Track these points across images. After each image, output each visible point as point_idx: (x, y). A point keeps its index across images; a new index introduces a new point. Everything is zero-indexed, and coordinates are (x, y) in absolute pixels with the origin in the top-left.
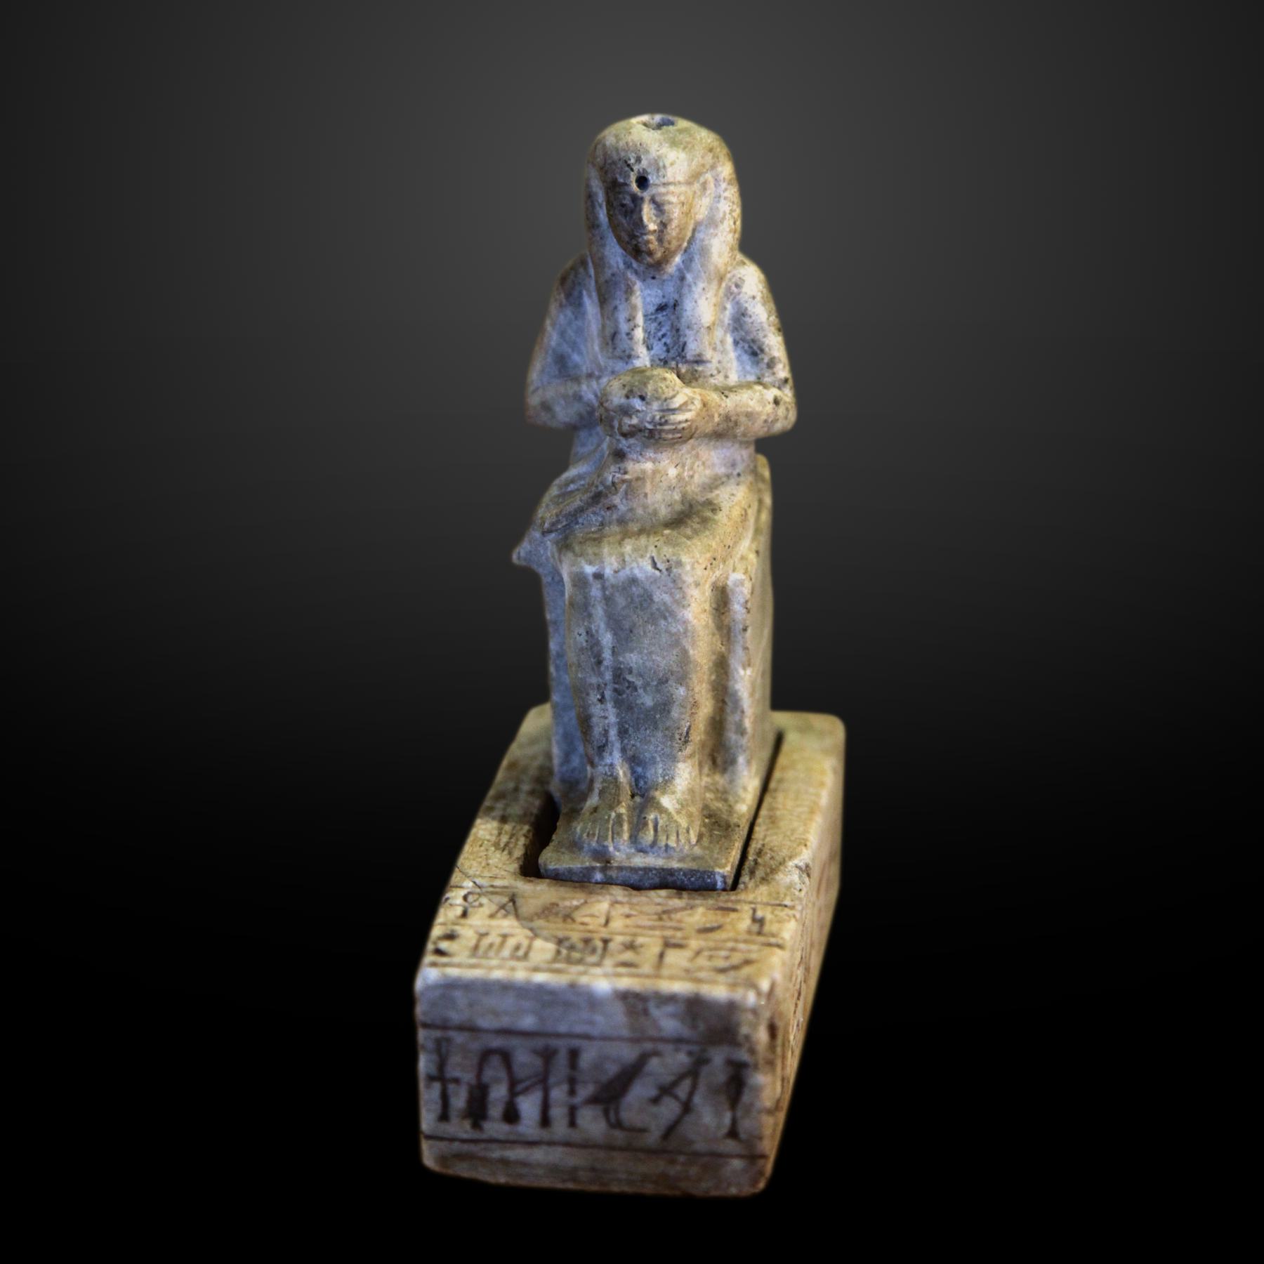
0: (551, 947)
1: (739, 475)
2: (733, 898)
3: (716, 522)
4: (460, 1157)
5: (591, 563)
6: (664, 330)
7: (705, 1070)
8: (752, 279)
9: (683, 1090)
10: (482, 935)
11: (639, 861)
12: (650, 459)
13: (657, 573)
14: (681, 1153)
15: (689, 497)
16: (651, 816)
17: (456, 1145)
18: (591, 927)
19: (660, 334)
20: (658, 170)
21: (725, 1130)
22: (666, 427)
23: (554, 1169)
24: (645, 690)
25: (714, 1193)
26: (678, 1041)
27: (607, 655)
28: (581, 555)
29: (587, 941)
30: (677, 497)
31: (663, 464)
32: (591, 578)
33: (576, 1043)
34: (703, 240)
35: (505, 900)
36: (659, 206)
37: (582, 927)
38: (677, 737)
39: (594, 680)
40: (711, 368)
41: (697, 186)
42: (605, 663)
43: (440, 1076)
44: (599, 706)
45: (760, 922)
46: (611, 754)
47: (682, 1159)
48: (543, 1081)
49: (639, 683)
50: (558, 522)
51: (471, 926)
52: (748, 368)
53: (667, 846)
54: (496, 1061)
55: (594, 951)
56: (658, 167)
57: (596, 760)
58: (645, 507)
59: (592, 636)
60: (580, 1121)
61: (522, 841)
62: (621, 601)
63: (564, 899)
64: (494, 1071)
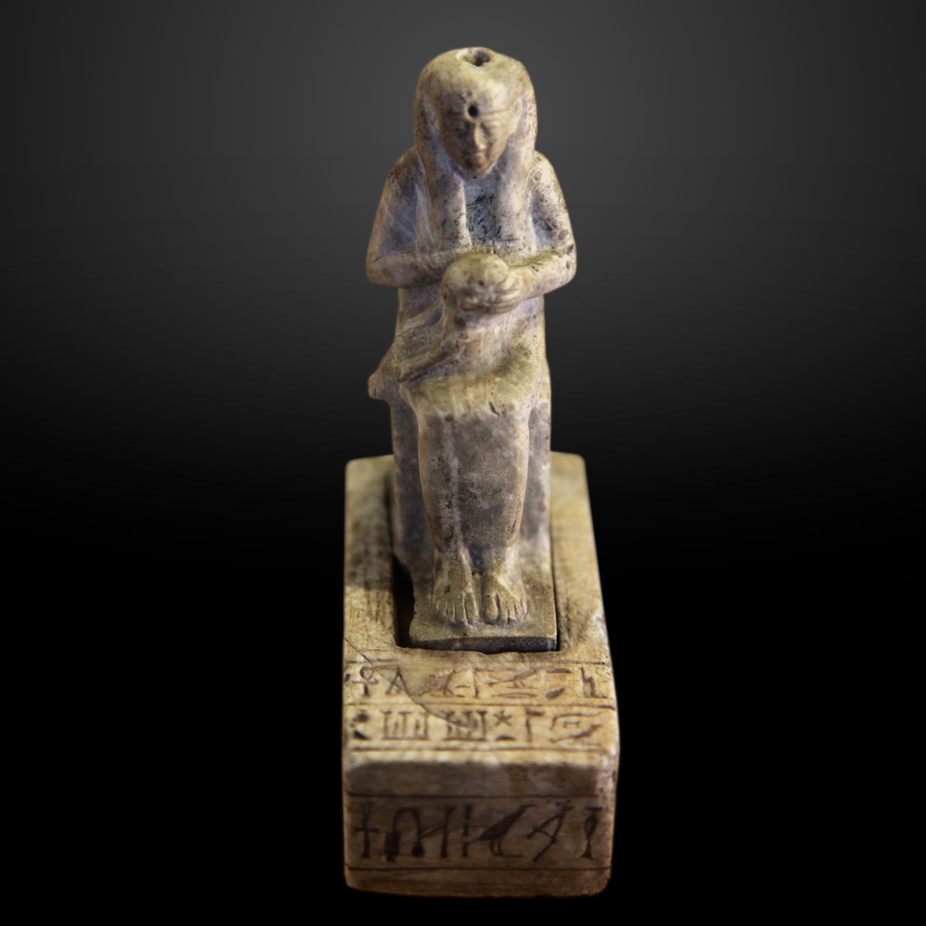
0: (442, 722)
2: (563, 658)
3: (530, 366)
5: (443, 409)
6: (482, 216)
7: (568, 814)
8: (546, 171)
10: (388, 713)
11: (489, 632)
12: (483, 325)
13: (495, 415)
14: (546, 869)
15: (506, 345)
16: (493, 595)
17: (374, 873)
18: (467, 700)
19: (479, 219)
24: (483, 498)
25: (572, 894)
26: (549, 796)
27: (454, 474)
28: (435, 402)
29: (468, 714)
30: (499, 347)
31: (492, 326)
32: (443, 421)
34: (514, 149)
35: (394, 675)
36: (487, 130)
37: (459, 700)
38: (506, 529)
39: (444, 492)
40: (519, 244)
42: (453, 480)
44: (447, 510)
45: (589, 681)
46: (456, 543)
47: (547, 873)
48: (444, 828)
49: (479, 493)
50: (412, 373)
51: (376, 705)
52: (544, 240)
53: (509, 619)
55: (475, 725)
56: (486, 100)
57: (444, 547)
58: (478, 359)
59: (443, 461)
60: (470, 852)
61: (388, 609)
62: (466, 436)
63: (437, 670)
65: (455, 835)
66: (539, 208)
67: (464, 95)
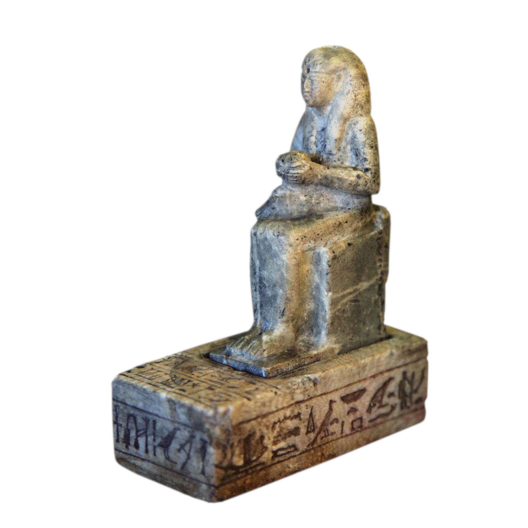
1: (349, 209)
7: (194, 440)
9: (187, 448)
20: (314, 65)
21: (200, 471)
22: (289, 175)
27: (257, 270)
33: (156, 418)
41: (335, 76)
49: (267, 285)
54: (132, 419)
62: (262, 247)
66: (354, 142)
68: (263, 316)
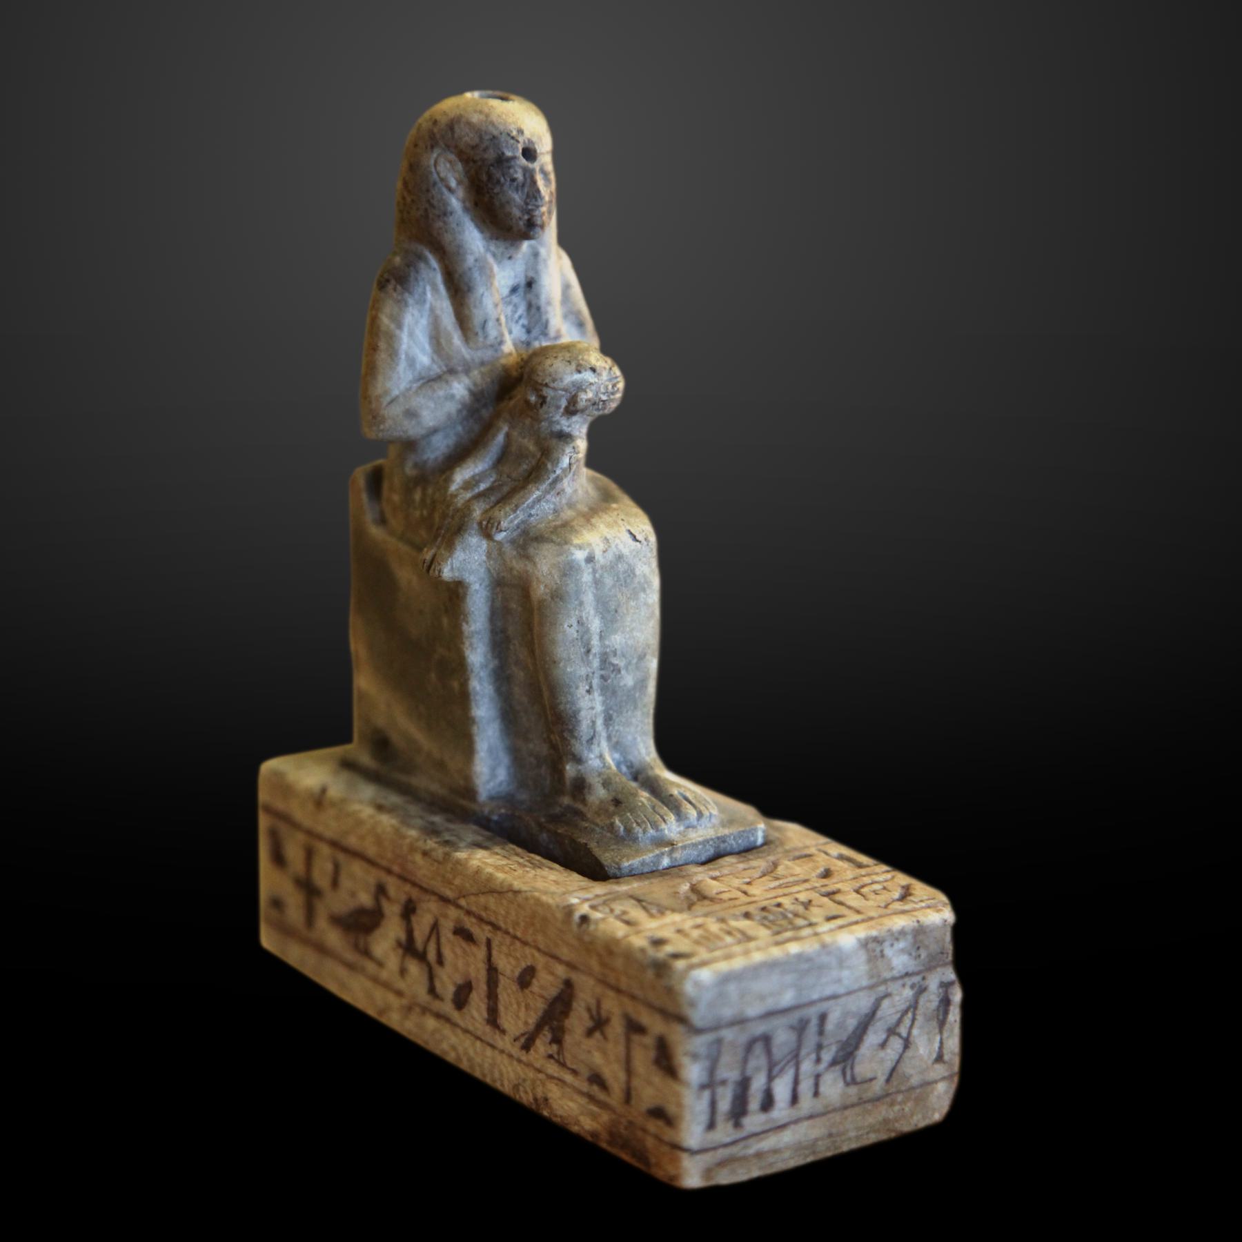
4: (722, 1164)
19: (516, 316)
23: (798, 1148)
43: (710, 1084)
44: (587, 697)
64: (758, 1060)
65: (807, 1066)
67: (514, 133)
68: (614, 740)
